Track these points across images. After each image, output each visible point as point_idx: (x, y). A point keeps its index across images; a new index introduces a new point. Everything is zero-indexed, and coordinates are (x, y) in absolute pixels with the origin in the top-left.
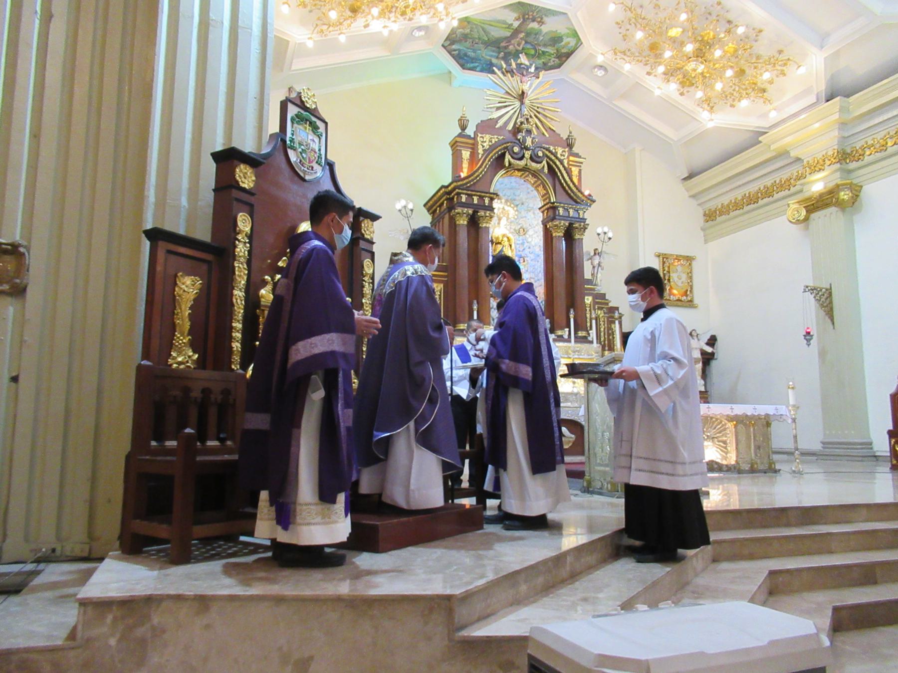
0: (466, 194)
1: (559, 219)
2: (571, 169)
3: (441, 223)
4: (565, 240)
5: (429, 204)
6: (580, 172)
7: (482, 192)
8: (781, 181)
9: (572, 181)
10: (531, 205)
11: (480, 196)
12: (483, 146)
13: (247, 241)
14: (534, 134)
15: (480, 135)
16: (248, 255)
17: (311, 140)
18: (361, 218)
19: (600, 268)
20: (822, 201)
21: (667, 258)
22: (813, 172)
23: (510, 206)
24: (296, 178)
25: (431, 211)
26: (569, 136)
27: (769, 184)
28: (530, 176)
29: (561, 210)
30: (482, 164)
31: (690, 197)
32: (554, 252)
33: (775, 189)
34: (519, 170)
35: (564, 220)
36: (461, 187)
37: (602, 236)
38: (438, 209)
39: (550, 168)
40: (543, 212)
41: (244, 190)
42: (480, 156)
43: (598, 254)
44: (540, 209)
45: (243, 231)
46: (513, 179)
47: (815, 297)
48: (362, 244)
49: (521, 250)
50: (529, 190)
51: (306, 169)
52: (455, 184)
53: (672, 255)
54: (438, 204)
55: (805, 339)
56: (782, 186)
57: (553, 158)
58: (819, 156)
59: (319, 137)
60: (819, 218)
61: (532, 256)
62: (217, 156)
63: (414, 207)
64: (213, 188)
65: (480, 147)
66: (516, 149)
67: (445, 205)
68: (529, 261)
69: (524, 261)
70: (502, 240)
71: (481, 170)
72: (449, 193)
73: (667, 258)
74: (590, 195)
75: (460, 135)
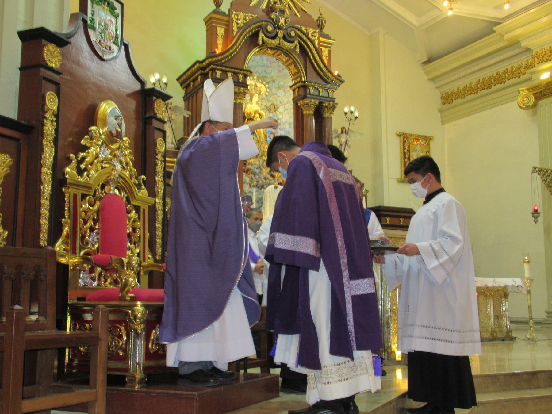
0: (220, 70)
2: (321, 49)
3: (194, 98)
4: (315, 118)
5: (182, 79)
6: (330, 52)
7: (236, 69)
8: (513, 69)
9: (322, 61)
10: (282, 83)
11: (234, 73)
12: (238, 24)
13: (54, 119)
14: (287, 14)
15: (234, 13)
16: (55, 134)
17: (108, 20)
18: (154, 98)
19: (347, 146)
20: (549, 89)
21: (407, 138)
22: (541, 62)
23: (262, 83)
24: (96, 58)
25: (184, 86)
26: (319, 17)
27: (501, 71)
28: (283, 55)
29: (311, 88)
30: (236, 42)
32: (304, 129)
34: (271, 49)
35: (314, 99)
36: (216, 63)
37: (349, 115)
38: (192, 83)
39: (301, 47)
40: (294, 90)
41: (51, 69)
42: (234, 33)
43: (345, 132)
44: (291, 87)
45: (51, 110)
46: (265, 57)
47: (542, 178)
48: (155, 123)
50: (280, 69)
51: (104, 49)
53: (411, 135)
54: (192, 79)
55: (533, 216)
56: (513, 73)
57: (305, 38)
59: (116, 17)
60: (546, 104)
62: (24, 36)
63: (168, 81)
64: (19, 65)
65: (235, 24)
66: (270, 28)
67: (199, 80)
70: (254, 116)
71: (235, 47)
72: (204, 68)
73: (407, 138)
74: (338, 75)
75: (214, 12)
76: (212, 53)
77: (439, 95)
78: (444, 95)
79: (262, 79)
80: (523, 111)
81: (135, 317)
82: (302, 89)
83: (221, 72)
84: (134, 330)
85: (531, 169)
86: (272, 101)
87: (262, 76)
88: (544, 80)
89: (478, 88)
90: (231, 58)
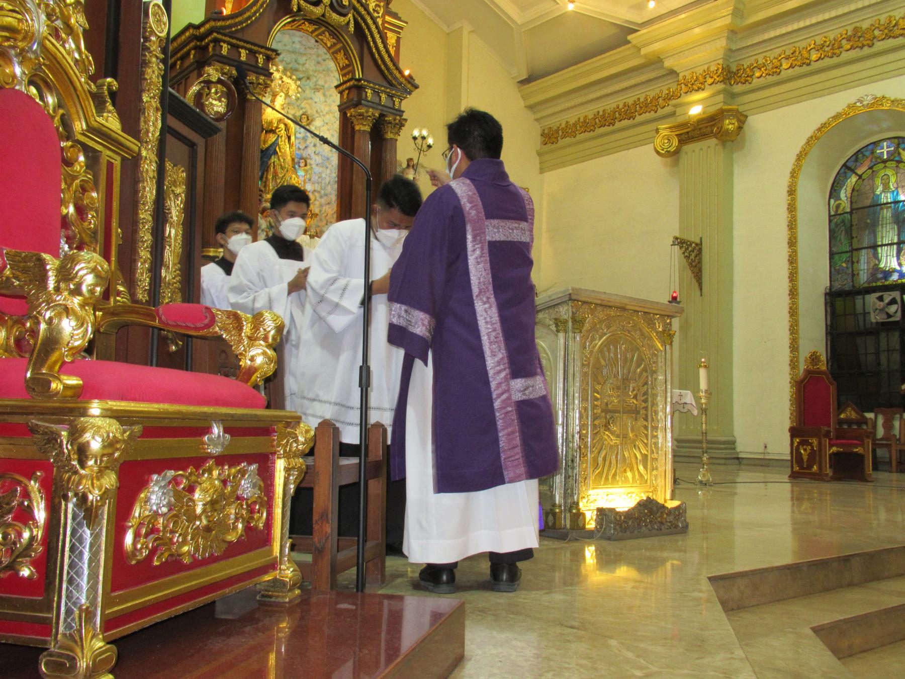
0: (229, 43)
1: (366, 106)
6: (398, 40)
7: (255, 45)
9: (388, 51)
10: (321, 82)
11: (250, 51)
20: (700, 129)
22: (690, 91)
23: (291, 78)
27: (630, 101)
28: (327, 34)
29: (369, 91)
31: (526, 107)
33: (638, 109)
34: (311, 22)
35: (373, 108)
37: (419, 141)
38: (179, 62)
39: (357, 25)
40: (341, 93)
43: (413, 167)
44: (337, 87)
47: (684, 253)
49: (302, 147)
50: (320, 59)
52: (212, 23)
54: (179, 55)
56: (647, 105)
57: (363, 12)
58: (700, 70)
60: (701, 149)
61: (318, 159)
67: (192, 56)
68: (314, 166)
69: (306, 165)
70: (277, 128)
71: (255, 9)
74: (410, 76)
76: (216, 13)
77: (539, 131)
78: (546, 131)
79: (290, 71)
80: (658, 158)
81: (82, 452)
82: (354, 92)
83: (229, 47)
84: (76, 495)
85: (672, 239)
86: (305, 108)
87: (291, 68)
88: (694, 116)
89: (596, 124)
90: (247, 26)
